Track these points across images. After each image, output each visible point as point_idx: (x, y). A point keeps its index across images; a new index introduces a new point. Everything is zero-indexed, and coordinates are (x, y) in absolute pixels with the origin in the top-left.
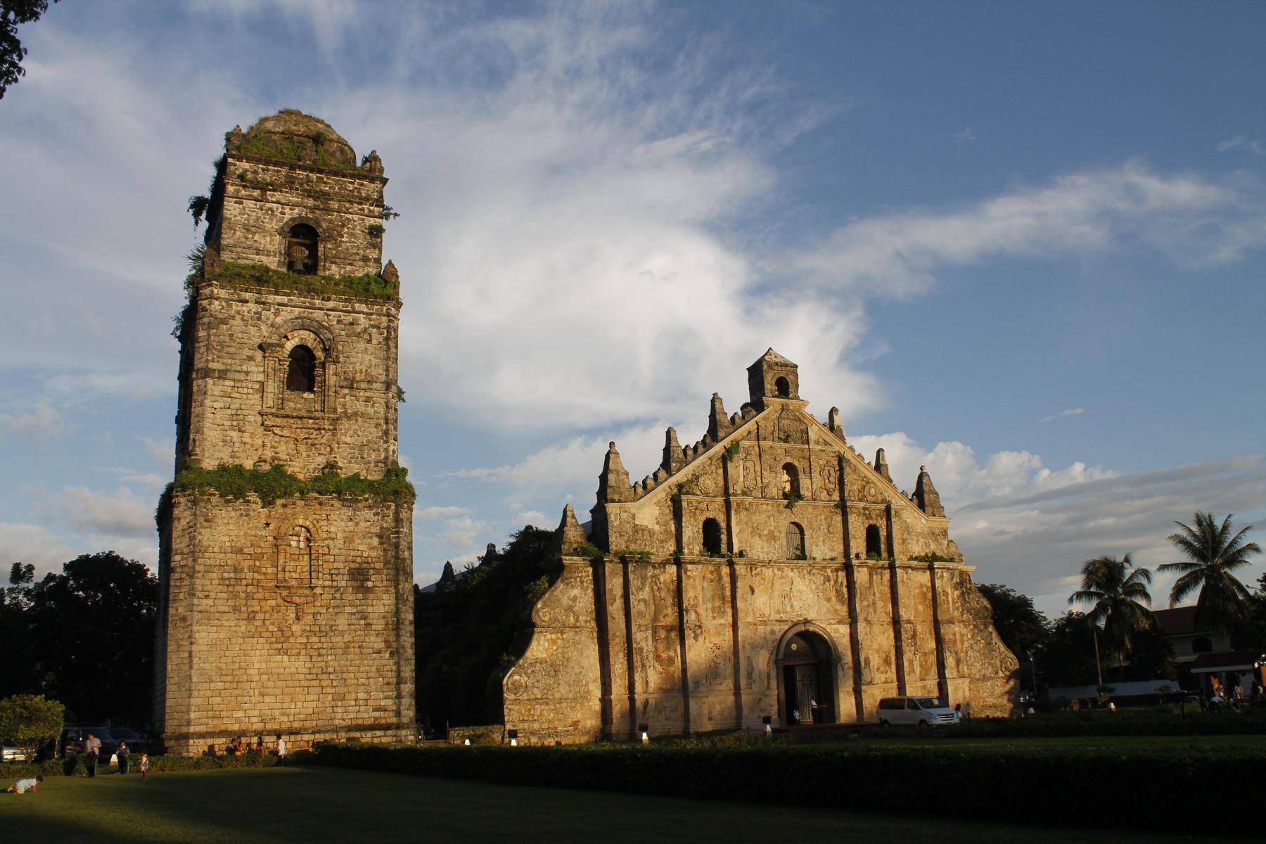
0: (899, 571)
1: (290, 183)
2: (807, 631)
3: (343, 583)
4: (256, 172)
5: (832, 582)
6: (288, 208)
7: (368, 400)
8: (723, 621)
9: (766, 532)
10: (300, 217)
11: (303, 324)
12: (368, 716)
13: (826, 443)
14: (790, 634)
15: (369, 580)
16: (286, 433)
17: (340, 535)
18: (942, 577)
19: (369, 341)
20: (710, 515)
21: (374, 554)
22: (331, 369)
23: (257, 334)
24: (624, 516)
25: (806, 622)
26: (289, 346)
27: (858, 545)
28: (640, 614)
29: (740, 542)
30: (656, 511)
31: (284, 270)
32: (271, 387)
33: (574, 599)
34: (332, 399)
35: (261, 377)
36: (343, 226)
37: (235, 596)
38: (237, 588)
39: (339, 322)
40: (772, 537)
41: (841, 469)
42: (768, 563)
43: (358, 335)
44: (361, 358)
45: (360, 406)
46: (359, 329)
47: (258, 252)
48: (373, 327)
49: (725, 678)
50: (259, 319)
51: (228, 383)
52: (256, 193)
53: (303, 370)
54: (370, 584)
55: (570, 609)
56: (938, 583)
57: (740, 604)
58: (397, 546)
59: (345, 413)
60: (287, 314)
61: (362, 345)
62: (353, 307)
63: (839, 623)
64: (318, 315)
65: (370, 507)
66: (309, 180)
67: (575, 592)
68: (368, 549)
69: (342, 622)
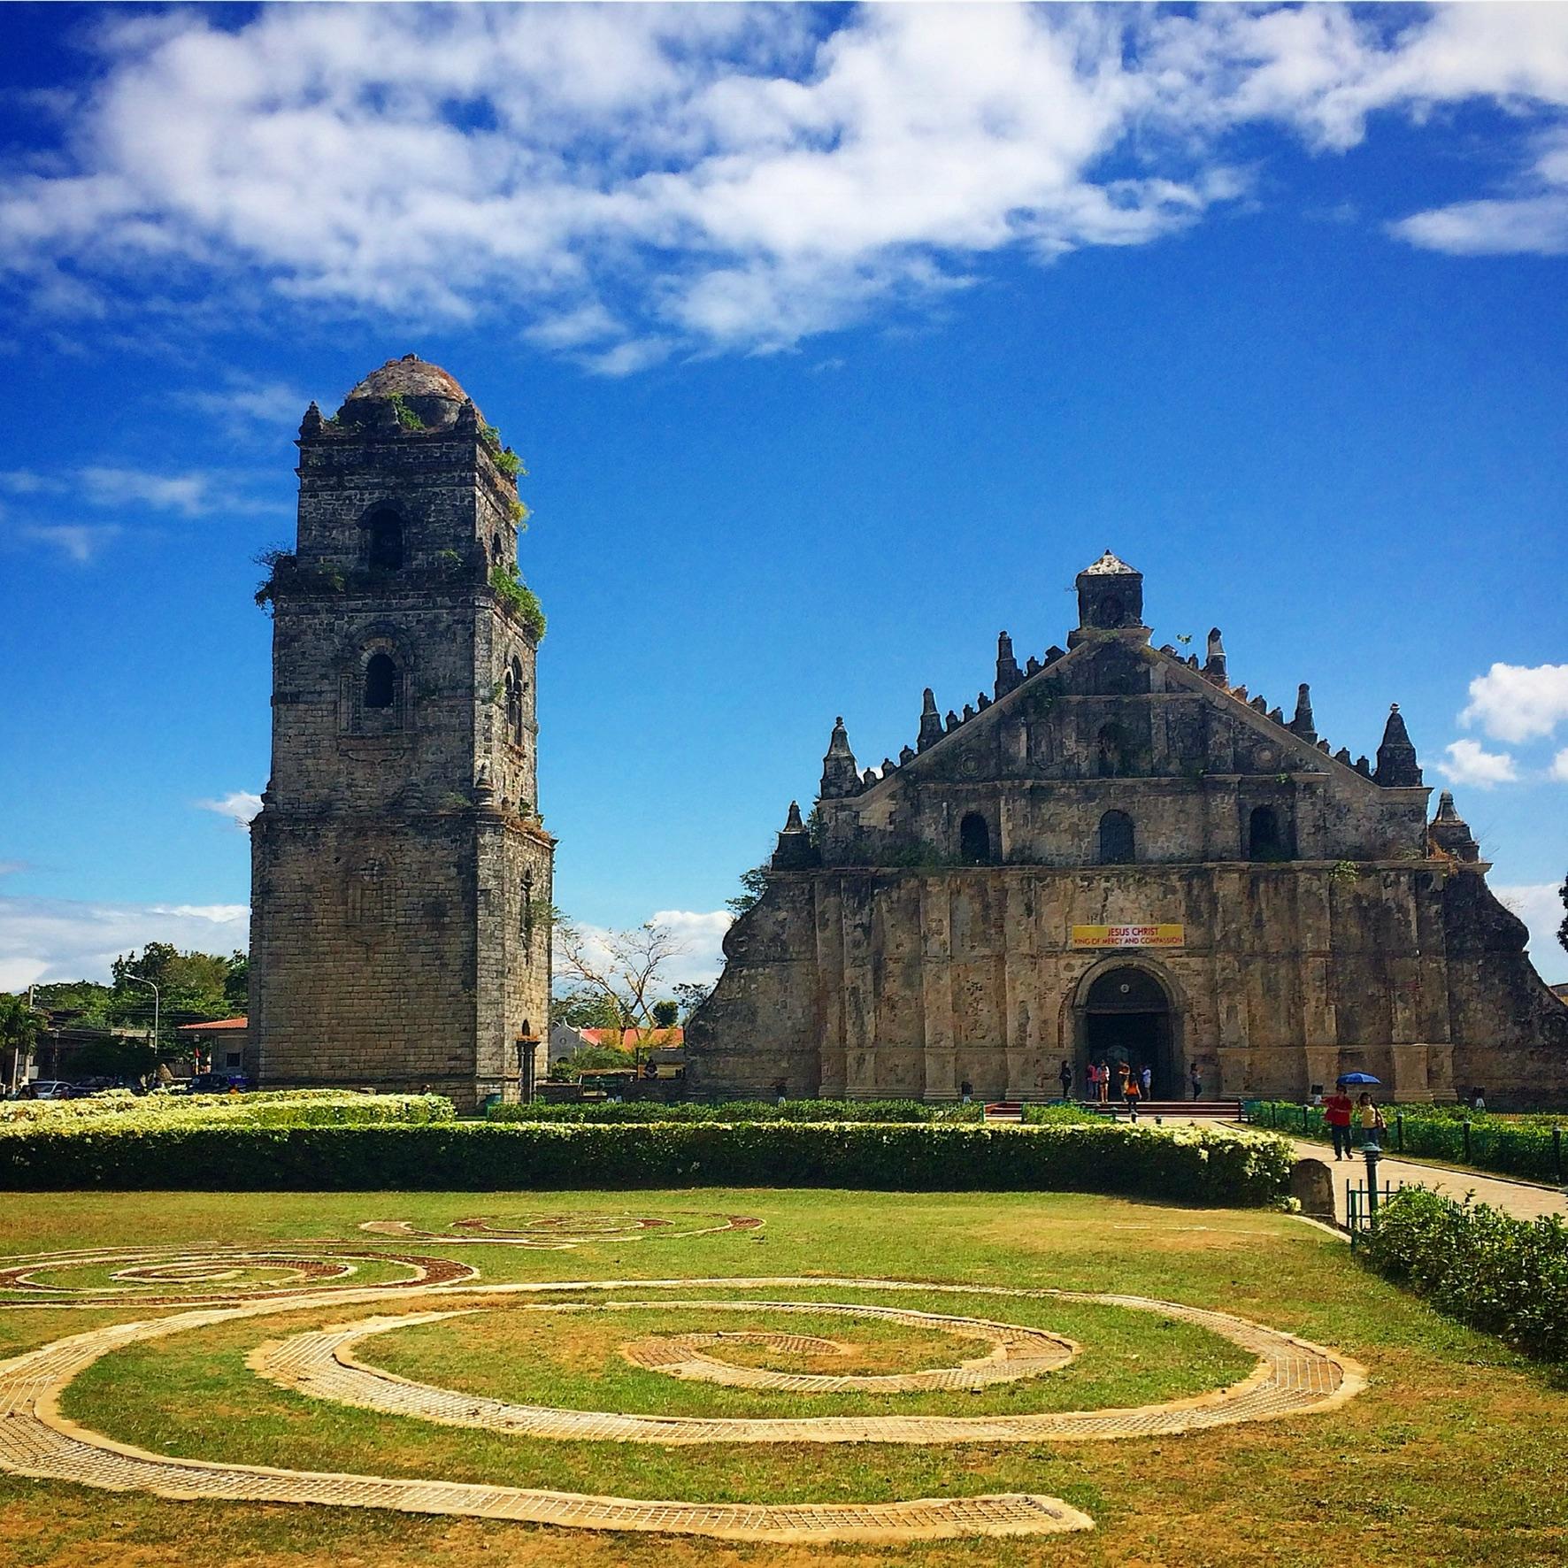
0: (1302, 877)
1: (368, 460)
2: (1127, 967)
3: (417, 920)
4: (330, 457)
5: (1181, 895)
6: (365, 494)
7: (452, 709)
8: (987, 952)
9: (1065, 825)
10: (380, 502)
11: (378, 629)
12: (443, 1065)
13: (1184, 688)
14: (1098, 971)
15: (445, 915)
16: (362, 756)
17: (414, 867)
18: (1397, 882)
19: (454, 640)
20: (973, 807)
21: (451, 885)
22: (408, 680)
23: (328, 649)
24: (842, 815)
25: (1127, 951)
26: (366, 656)
27: (1228, 836)
28: (857, 944)
29: (1014, 841)
30: (890, 806)
31: (365, 568)
32: (344, 706)
33: (782, 924)
34: (410, 713)
35: (330, 697)
36: (430, 502)
37: (306, 936)
38: (308, 929)
39: (418, 622)
40: (1077, 834)
41: (1205, 725)
42: (1066, 870)
43: (442, 635)
44: (442, 663)
45: (444, 718)
46: (441, 627)
47: (336, 551)
48: (457, 622)
49: (989, 1030)
50: (332, 631)
51: (302, 707)
52: (333, 481)
53: (382, 684)
54: (447, 920)
55: (775, 938)
56: (1387, 894)
57: (1009, 928)
58: (475, 877)
59: (427, 727)
60: (361, 620)
61: (445, 646)
62: (435, 603)
63: (1188, 955)
64: (396, 616)
65: (447, 834)
66: (390, 452)
67: (783, 915)
68: (444, 880)
69: (415, 962)
